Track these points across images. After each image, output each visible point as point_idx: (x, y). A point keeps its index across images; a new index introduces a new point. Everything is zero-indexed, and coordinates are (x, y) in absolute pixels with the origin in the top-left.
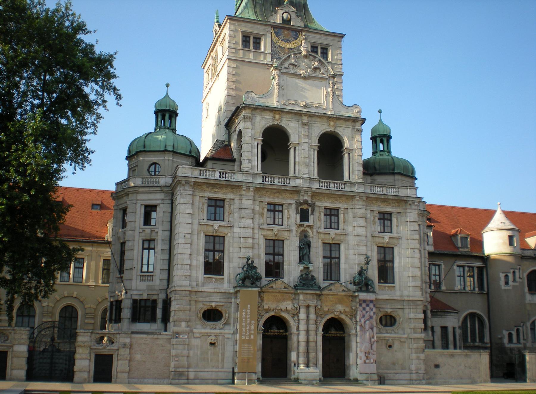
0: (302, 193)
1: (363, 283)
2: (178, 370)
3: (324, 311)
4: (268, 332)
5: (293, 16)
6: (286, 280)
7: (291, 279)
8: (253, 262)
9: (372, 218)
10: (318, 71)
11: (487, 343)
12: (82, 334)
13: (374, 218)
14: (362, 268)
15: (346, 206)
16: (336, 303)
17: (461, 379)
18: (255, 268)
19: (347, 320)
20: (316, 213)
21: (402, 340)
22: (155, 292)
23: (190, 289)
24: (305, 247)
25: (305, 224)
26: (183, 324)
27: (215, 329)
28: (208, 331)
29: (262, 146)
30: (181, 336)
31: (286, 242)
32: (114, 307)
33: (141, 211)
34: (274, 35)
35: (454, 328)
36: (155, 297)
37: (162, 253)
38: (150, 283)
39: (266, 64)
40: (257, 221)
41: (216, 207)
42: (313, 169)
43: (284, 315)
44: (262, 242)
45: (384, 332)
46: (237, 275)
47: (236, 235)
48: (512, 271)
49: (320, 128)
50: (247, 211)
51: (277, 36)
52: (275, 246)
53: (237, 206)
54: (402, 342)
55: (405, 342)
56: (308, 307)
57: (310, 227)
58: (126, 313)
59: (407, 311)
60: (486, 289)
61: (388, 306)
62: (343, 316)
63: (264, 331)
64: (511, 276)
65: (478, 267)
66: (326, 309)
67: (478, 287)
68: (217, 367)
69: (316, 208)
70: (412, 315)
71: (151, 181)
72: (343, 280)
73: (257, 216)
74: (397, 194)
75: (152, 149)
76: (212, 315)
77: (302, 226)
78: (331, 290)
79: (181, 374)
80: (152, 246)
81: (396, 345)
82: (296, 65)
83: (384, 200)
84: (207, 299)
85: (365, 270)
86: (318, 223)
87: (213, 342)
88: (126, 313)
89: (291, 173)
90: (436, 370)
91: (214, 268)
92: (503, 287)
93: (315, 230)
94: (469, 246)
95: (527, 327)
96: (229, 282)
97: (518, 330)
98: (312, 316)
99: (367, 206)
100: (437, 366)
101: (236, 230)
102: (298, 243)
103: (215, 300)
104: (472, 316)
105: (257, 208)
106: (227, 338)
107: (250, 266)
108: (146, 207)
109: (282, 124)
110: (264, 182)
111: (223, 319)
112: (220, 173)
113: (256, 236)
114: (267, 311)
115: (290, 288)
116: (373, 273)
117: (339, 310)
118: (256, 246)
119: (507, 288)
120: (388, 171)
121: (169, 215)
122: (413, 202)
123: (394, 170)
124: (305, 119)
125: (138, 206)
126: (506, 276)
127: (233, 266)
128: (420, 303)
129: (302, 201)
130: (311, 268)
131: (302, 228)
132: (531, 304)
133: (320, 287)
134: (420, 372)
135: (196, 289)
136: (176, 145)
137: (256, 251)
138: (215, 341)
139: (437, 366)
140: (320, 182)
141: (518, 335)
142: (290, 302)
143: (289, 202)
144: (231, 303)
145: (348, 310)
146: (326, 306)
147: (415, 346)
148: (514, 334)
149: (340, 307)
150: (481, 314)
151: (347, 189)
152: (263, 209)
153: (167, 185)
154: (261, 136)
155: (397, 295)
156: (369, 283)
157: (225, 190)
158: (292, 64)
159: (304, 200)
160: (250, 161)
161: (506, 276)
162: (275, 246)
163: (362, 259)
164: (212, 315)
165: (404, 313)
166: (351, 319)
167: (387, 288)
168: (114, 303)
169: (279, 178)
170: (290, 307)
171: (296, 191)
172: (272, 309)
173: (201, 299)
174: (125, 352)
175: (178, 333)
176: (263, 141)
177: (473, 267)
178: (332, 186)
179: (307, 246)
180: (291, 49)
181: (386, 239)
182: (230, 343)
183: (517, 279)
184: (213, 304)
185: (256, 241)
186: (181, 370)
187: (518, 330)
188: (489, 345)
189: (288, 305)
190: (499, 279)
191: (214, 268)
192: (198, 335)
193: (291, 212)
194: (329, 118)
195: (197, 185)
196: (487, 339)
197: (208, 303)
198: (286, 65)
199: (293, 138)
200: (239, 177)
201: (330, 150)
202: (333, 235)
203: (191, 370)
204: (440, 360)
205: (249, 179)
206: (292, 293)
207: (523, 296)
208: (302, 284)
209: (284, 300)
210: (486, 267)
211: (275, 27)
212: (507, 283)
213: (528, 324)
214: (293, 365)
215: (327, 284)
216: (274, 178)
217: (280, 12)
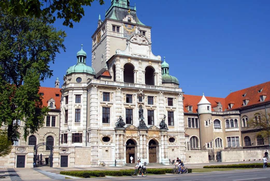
0: (140, 90)
1: (163, 126)
2: (94, 161)
3: (150, 137)
4: (128, 145)
5: (132, 19)
6: (134, 125)
7: (136, 124)
8: (122, 118)
9: (166, 100)
10: (144, 42)
11: (199, 148)
12: (55, 148)
13: (166, 100)
14: (163, 120)
15: (156, 96)
16: (153, 134)
18: (123, 120)
19: (158, 140)
20: (145, 98)
22: (82, 130)
23: (97, 129)
24: (141, 112)
25: (141, 102)
26: (95, 143)
27: (107, 145)
28: (105, 145)
29: (124, 71)
30: (95, 148)
31: (133, 110)
32: (63, 137)
33: (74, 97)
34: (125, 26)
35: (188, 142)
36: (81, 132)
37: (84, 114)
38: (79, 127)
39: (122, 38)
41: (106, 96)
42: (143, 81)
43: (134, 138)
44: (125, 110)
45: (171, 144)
46: (116, 123)
47: (115, 107)
48: (209, 120)
49: (146, 64)
50: (119, 97)
51: (126, 27)
52: (129, 112)
53: (115, 95)
56: (143, 135)
57: (143, 104)
58: (70, 139)
59: (179, 136)
60: (199, 127)
61: (172, 135)
62: (156, 139)
63: (127, 145)
64: (208, 122)
65: (196, 119)
66: (150, 136)
67: (196, 126)
68: (109, 160)
69: (145, 96)
70: (181, 138)
71: (79, 85)
72: (155, 125)
73: (122, 100)
74: (175, 91)
75: (78, 72)
76: (106, 139)
77: (139, 103)
78: (151, 128)
79: (95, 163)
80: (79, 112)
81: (175, 149)
82: (136, 39)
83: (170, 93)
84: (104, 133)
85: (164, 121)
86: (146, 102)
87: (107, 150)
88: (70, 139)
89: (135, 82)
90: (190, 158)
91: (106, 120)
92: (205, 126)
93: (145, 105)
94: (192, 110)
95: (214, 141)
96: (112, 126)
97: (211, 142)
98: (145, 139)
99: (164, 96)
100: (190, 157)
102: (138, 111)
103: (107, 133)
104: (194, 137)
106: (112, 148)
107: (121, 119)
108: (76, 95)
109: (131, 63)
110: (125, 86)
111: (110, 141)
112: (108, 82)
113: (122, 108)
114: (127, 137)
115: (136, 128)
116: (166, 122)
117: (154, 136)
119: (207, 126)
120: (169, 82)
121: (86, 99)
122: (181, 94)
123: (171, 81)
124: (140, 61)
125: (73, 95)
126: (207, 122)
127: (114, 120)
129: (140, 94)
130: (144, 120)
131: (140, 104)
132: (215, 132)
133: (147, 128)
134: (184, 159)
135: (99, 129)
136: (87, 70)
138: (108, 150)
139: (190, 157)
140: (146, 86)
141: (211, 144)
142: (137, 134)
143: (135, 94)
144: (113, 134)
145: (158, 136)
147: (182, 150)
148: (210, 144)
150: (197, 136)
151: (156, 89)
152: (125, 97)
153: (85, 86)
154: (123, 67)
155: (175, 130)
156: (166, 126)
158: (135, 39)
159: (141, 93)
160: (119, 77)
161: (207, 122)
162: (129, 112)
163: (163, 117)
164: (106, 139)
165: (178, 137)
166: (159, 140)
168: (63, 135)
169: (130, 84)
170: (136, 136)
171: (137, 90)
172: (130, 136)
173: (101, 133)
174: (72, 155)
175: (93, 147)
176: (124, 69)
177: (190, 118)
178: (151, 88)
179: (142, 111)
180: (132, 32)
181: (171, 108)
182: (114, 150)
183: (211, 123)
184: (107, 135)
185: (122, 109)
186: (95, 161)
187: (211, 142)
188: (200, 149)
190: (204, 123)
191: (106, 120)
192: (101, 147)
193: (135, 98)
194: (148, 61)
195: (100, 87)
196: (199, 146)
197: (104, 135)
198: (132, 39)
199: (136, 68)
200: (115, 84)
201: (150, 74)
204: (191, 154)
205: (119, 84)
206: (137, 130)
207: (212, 130)
208: (140, 127)
209: (134, 133)
210: (199, 118)
211: (125, 23)
212: (207, 124)
213: (214, 140)
214: (138, 158)
215: (150, 126)
216: (129, 84)
217: (127, 17)
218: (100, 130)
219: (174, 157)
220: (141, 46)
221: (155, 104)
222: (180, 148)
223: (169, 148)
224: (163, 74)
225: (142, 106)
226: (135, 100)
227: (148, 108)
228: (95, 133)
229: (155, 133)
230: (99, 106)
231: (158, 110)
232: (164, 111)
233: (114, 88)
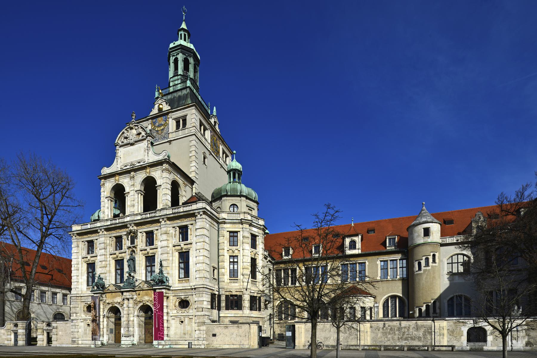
21: (191, 317)
25: (131, 246)
40: (108, 250)
66: (138, 300)
70: (196, 299)
81: (187, 321)
90: (214, 338)
100: (214, 335)
101: (98, 257)
105: (108, 242)
113: (108, 259)
114: (109, 304)
118: (108, 266)
137: (107, 269)
139: (214, 335)
147: (197, 321)
149: (146, 298)
157: (94, 235)
170: (119, 301)
189: (119, 299)
202: (148, 250)
219: (185, 334)
222: (194, 317)
224: (230, 183)
225: (133, 251)
226: (126, 243)
227: (143, 252)
229: (147, 295)
230: (80, 263)
231: (160, 253)
233: (95, 232)
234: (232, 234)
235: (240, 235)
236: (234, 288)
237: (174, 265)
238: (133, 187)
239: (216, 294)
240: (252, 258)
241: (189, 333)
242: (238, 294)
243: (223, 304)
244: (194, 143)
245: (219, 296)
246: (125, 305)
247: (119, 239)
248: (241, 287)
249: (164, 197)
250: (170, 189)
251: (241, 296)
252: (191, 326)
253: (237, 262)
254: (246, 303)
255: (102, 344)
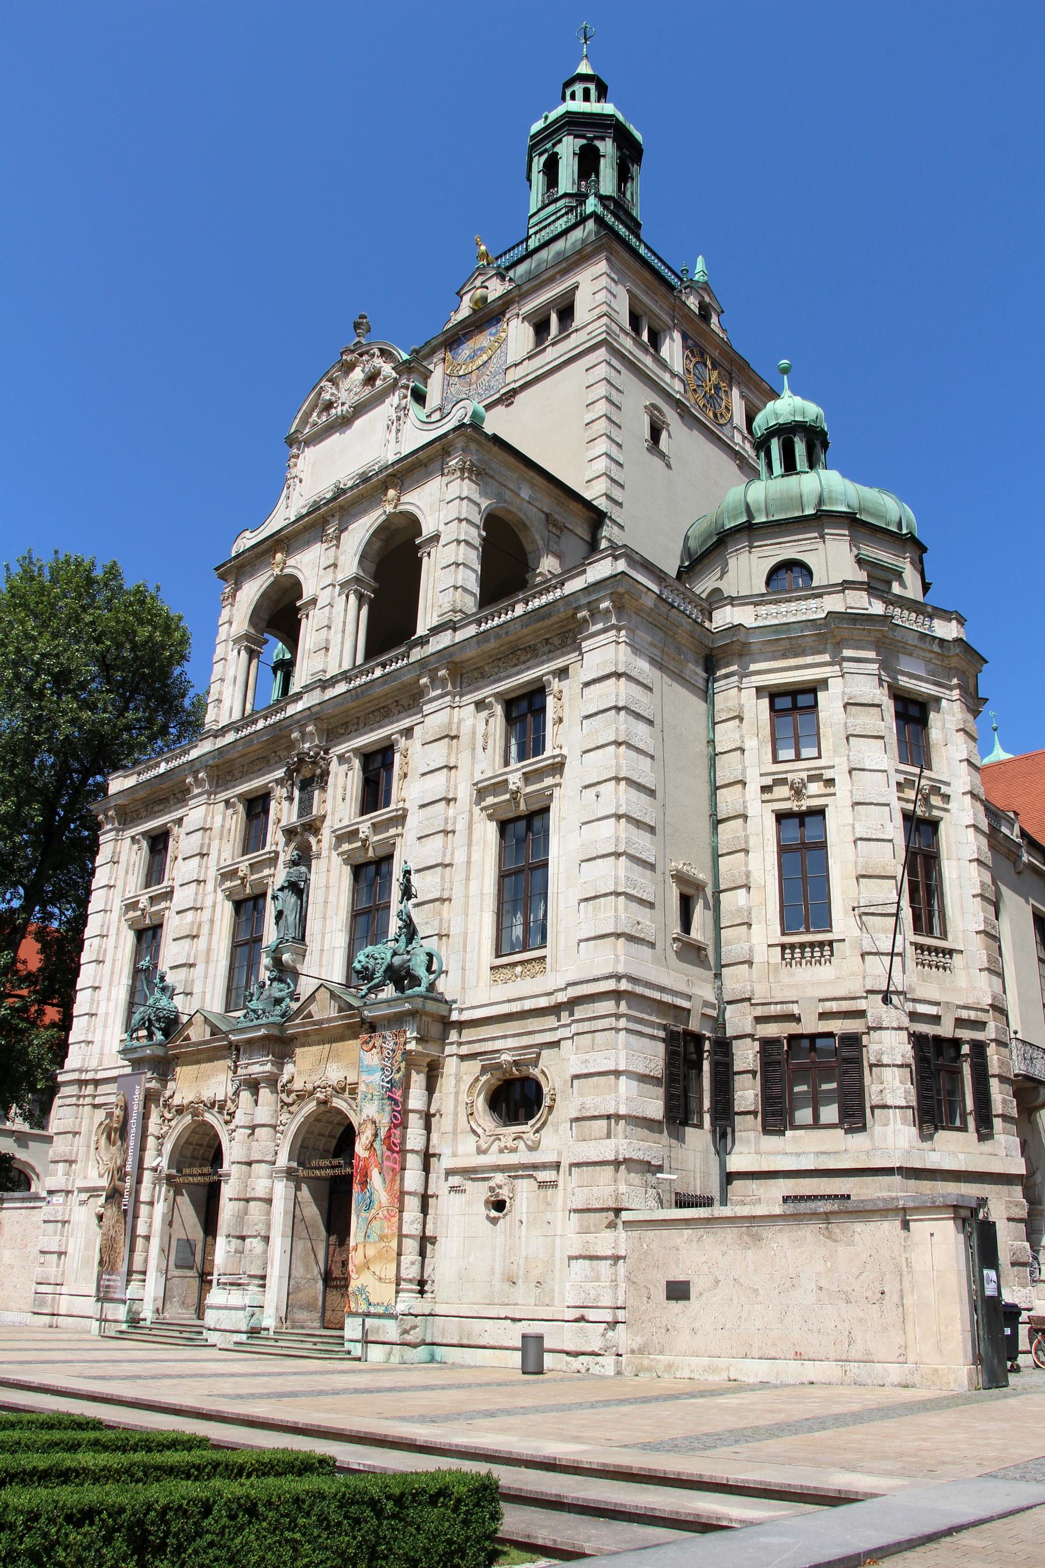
2: (42, 1289)
9: (481, 727)
15: (406, 723)
17: (798, 1356)
54: (543, 1185)
55: (553, 1184)
61: (511, 1043)
93: (326, 833)
100: (678, 1291)
118: (205, 928)
128: (607, 1006)
134: (590, 1314)
137: (202, 943)
139: (678, 1291)
146: (300, 1073)
167: (519, 969)
185: (206, 915)
203: (64, 1290)
218: (97, 1083)
220: (358, 423)
221: (403, 794)
223: (469, 1185)
226: (283, 812)
228: (68, 1101)
232: (461, 826)
234: (785, 702)
235: (829, 704)
236: (811, 991)
237: (473, 885)
238: (327, 574)
239: (698, 1039)
240: (908, 817)
241: (536, 1273)
242: (836, 1026)
243: (747, 1094)
244: (603, 370)
245: (723, 1046)
246: (240, 1119)
247: (256, 807)
248: (856, 987)
249: (447, 583)
250: (477, 542)
251: (853, 1041)
252: (549, 1228)
253: (822, 846)
254: (891, 1085)
255: (134, 1321)
